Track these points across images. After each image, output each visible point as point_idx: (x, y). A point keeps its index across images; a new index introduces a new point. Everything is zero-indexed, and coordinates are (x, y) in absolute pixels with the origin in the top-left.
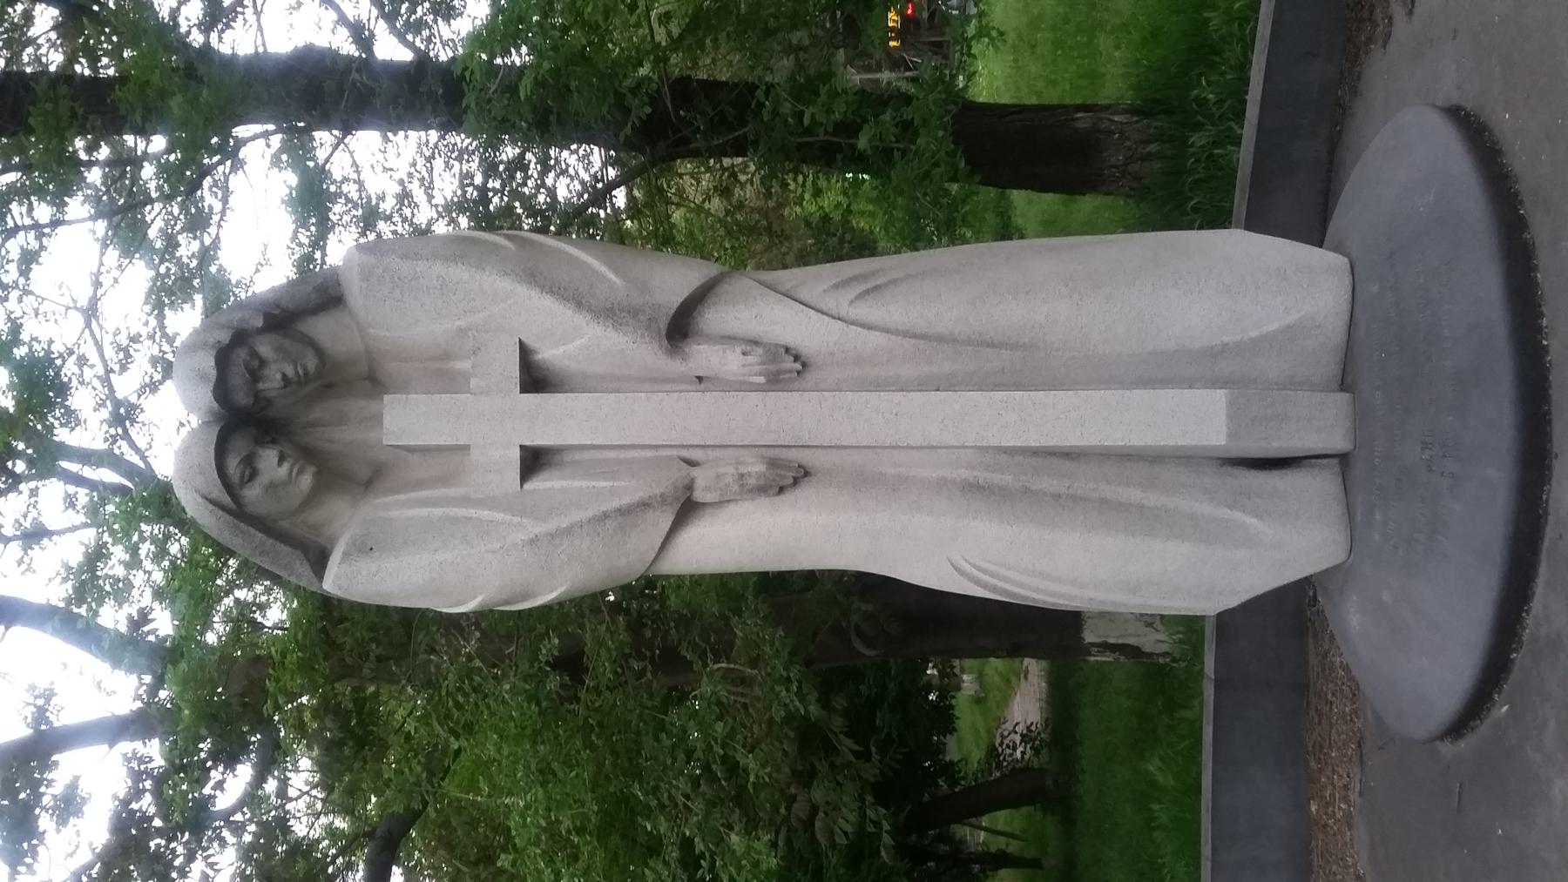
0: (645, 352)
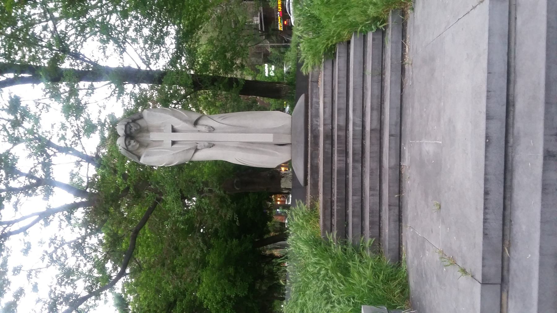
0: (190, 127)
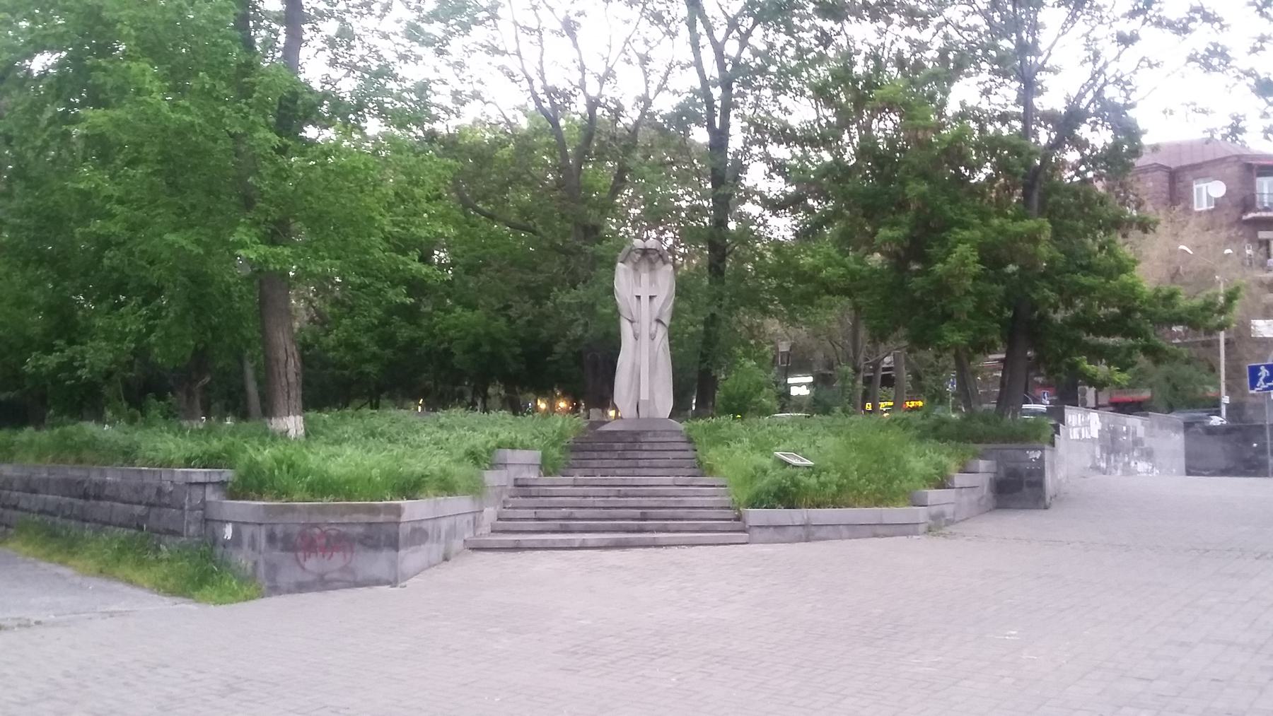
0: (655, 316)
